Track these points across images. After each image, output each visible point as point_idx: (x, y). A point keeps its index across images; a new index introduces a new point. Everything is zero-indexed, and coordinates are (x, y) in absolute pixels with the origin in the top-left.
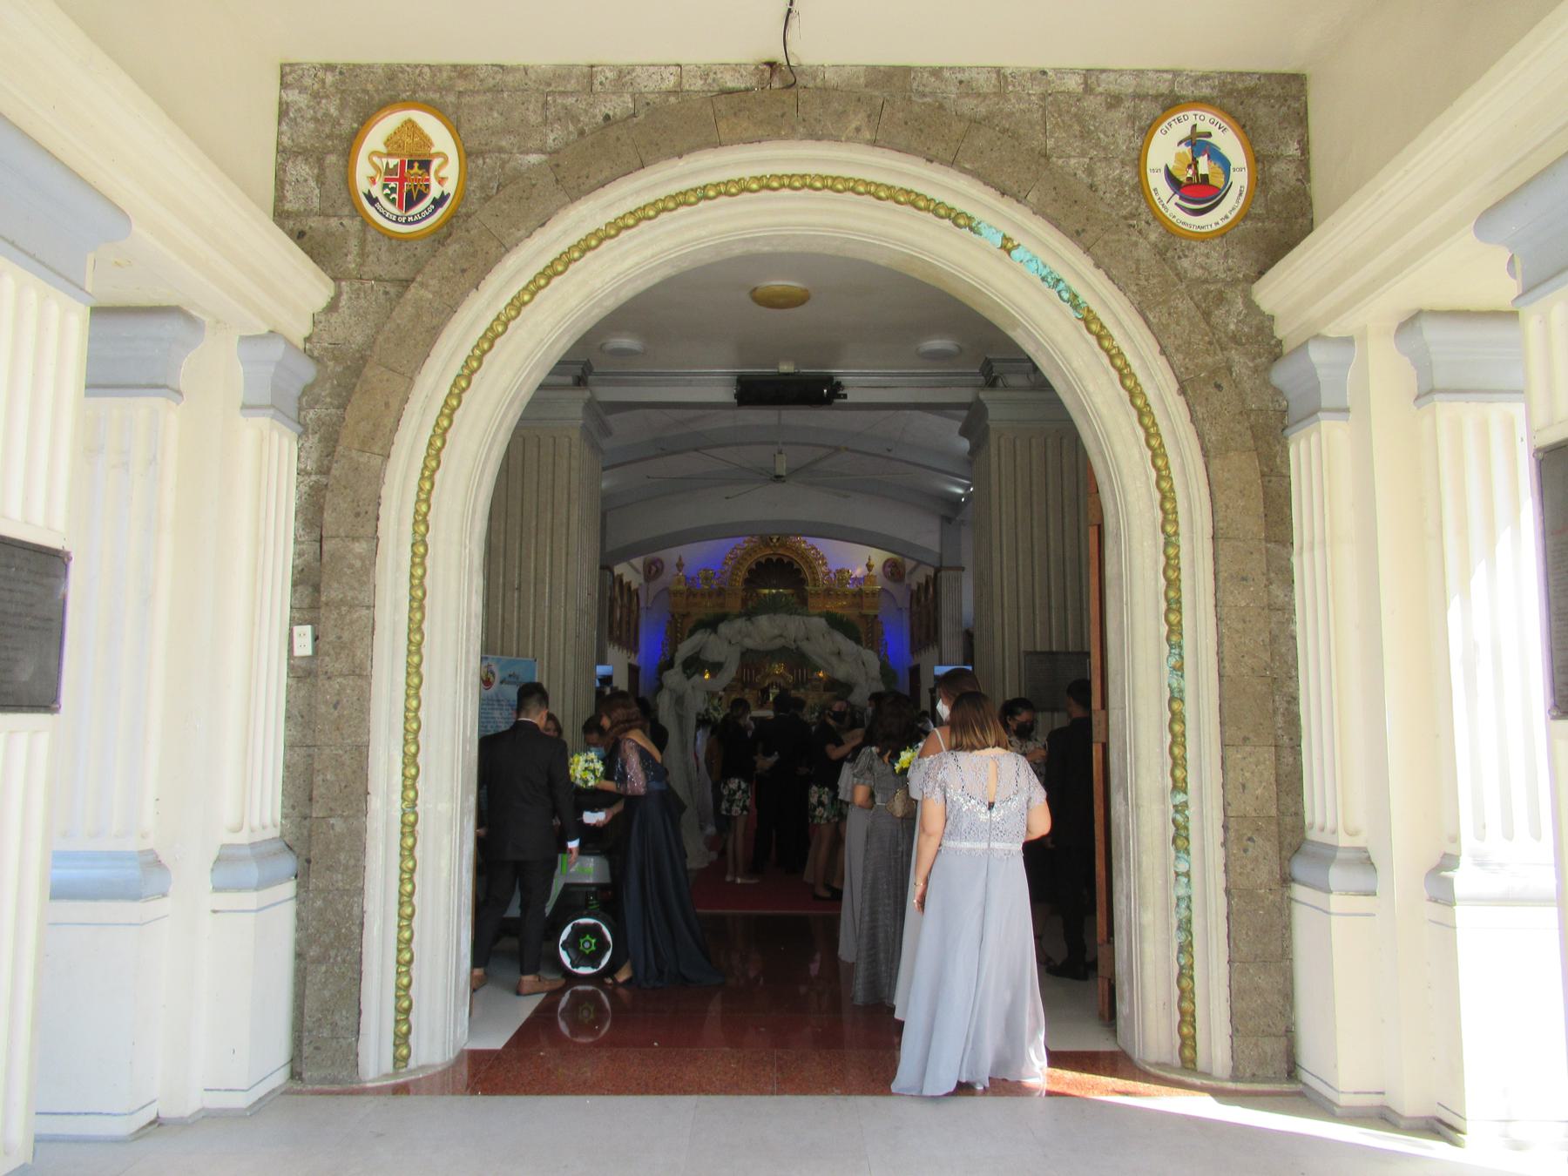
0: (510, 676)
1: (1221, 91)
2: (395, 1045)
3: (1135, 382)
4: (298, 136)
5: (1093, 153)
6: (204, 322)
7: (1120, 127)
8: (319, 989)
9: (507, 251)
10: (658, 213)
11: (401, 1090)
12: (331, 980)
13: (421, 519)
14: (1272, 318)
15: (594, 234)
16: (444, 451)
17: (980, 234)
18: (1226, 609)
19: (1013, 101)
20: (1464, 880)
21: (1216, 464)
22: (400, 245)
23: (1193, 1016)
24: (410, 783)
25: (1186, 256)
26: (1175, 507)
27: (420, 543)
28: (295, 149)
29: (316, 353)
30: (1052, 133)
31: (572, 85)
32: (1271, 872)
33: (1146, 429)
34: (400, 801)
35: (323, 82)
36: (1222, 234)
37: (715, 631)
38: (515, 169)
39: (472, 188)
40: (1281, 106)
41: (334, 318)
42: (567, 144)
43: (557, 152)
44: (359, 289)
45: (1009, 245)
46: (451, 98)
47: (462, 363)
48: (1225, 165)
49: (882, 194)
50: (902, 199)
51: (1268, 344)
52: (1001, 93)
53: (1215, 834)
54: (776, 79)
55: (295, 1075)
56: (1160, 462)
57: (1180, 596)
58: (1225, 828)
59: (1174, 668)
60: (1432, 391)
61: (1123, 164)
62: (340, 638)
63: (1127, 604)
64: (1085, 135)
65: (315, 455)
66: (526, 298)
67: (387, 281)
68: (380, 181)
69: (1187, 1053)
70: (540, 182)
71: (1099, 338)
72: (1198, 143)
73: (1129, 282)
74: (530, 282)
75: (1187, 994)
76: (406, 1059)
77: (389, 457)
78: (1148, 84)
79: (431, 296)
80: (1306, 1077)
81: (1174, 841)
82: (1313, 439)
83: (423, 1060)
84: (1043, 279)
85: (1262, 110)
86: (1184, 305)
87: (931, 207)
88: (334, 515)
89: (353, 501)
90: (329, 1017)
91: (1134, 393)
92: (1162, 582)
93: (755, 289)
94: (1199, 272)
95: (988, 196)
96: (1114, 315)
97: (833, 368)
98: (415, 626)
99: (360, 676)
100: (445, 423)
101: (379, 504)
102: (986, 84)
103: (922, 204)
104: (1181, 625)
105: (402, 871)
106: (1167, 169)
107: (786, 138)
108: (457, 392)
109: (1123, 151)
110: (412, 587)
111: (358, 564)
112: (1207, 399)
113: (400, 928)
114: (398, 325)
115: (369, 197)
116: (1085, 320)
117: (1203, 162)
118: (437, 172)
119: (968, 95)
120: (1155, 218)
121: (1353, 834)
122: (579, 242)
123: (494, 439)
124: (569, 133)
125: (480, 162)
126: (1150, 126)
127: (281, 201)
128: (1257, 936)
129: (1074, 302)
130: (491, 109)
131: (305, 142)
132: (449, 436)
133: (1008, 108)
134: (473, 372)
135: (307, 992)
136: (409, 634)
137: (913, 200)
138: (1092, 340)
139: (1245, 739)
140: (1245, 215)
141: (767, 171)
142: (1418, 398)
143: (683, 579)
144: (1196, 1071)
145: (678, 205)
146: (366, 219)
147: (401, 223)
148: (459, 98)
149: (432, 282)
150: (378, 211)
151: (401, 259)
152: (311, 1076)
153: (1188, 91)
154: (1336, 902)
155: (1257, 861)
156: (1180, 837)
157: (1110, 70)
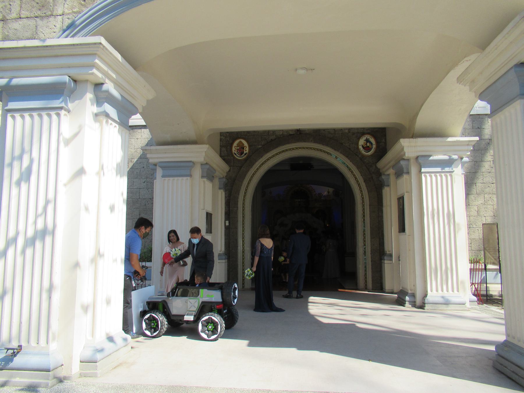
14: (380, 169)
24: (243, 245)
27: (243, 207)
35: (227, 135)
36: (371, 155)
46: (247, 137)
48: (372, 144)
53: (370, 252)
61: (355, 144)
69: (366, 287)
72: (367, 141)
84: (342, 163)
91: (357, 181)
103: (322, 151)
106: (362, 145)
115: (235, 153)
116: (349, 169)
121: (390, 251)
129: (347, 167)
137: (321, 150)
140: (375, 152)
141: (297, 147)
156: (365, 253)
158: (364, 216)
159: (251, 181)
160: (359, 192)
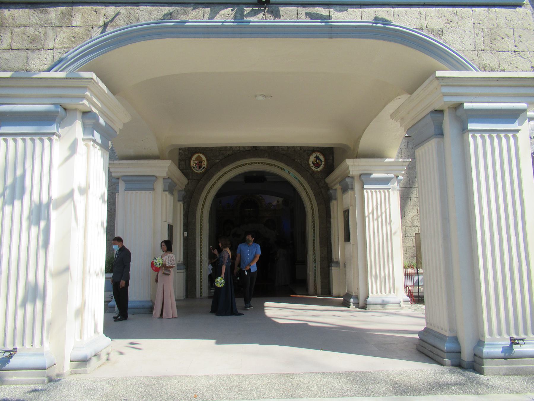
5: (301, 159)
13: (201, 215)
14: (328, 184)
24: (201, 255)
27: (201, 219)
36: (321, 171)
48: (321, 161)
69: (316, 292)
72: (317, 158)
81: (314, 262)
91: (308, 195)
92: (312, 223)
115: (193, 167)
116: (301, 184)
117: (318, 160)
121: (337, 259)
129: (299, 181)
137: (275, 166)
140: (324, 168)
141: (253, 162)
156: (315, 261)
158: (314, 227)
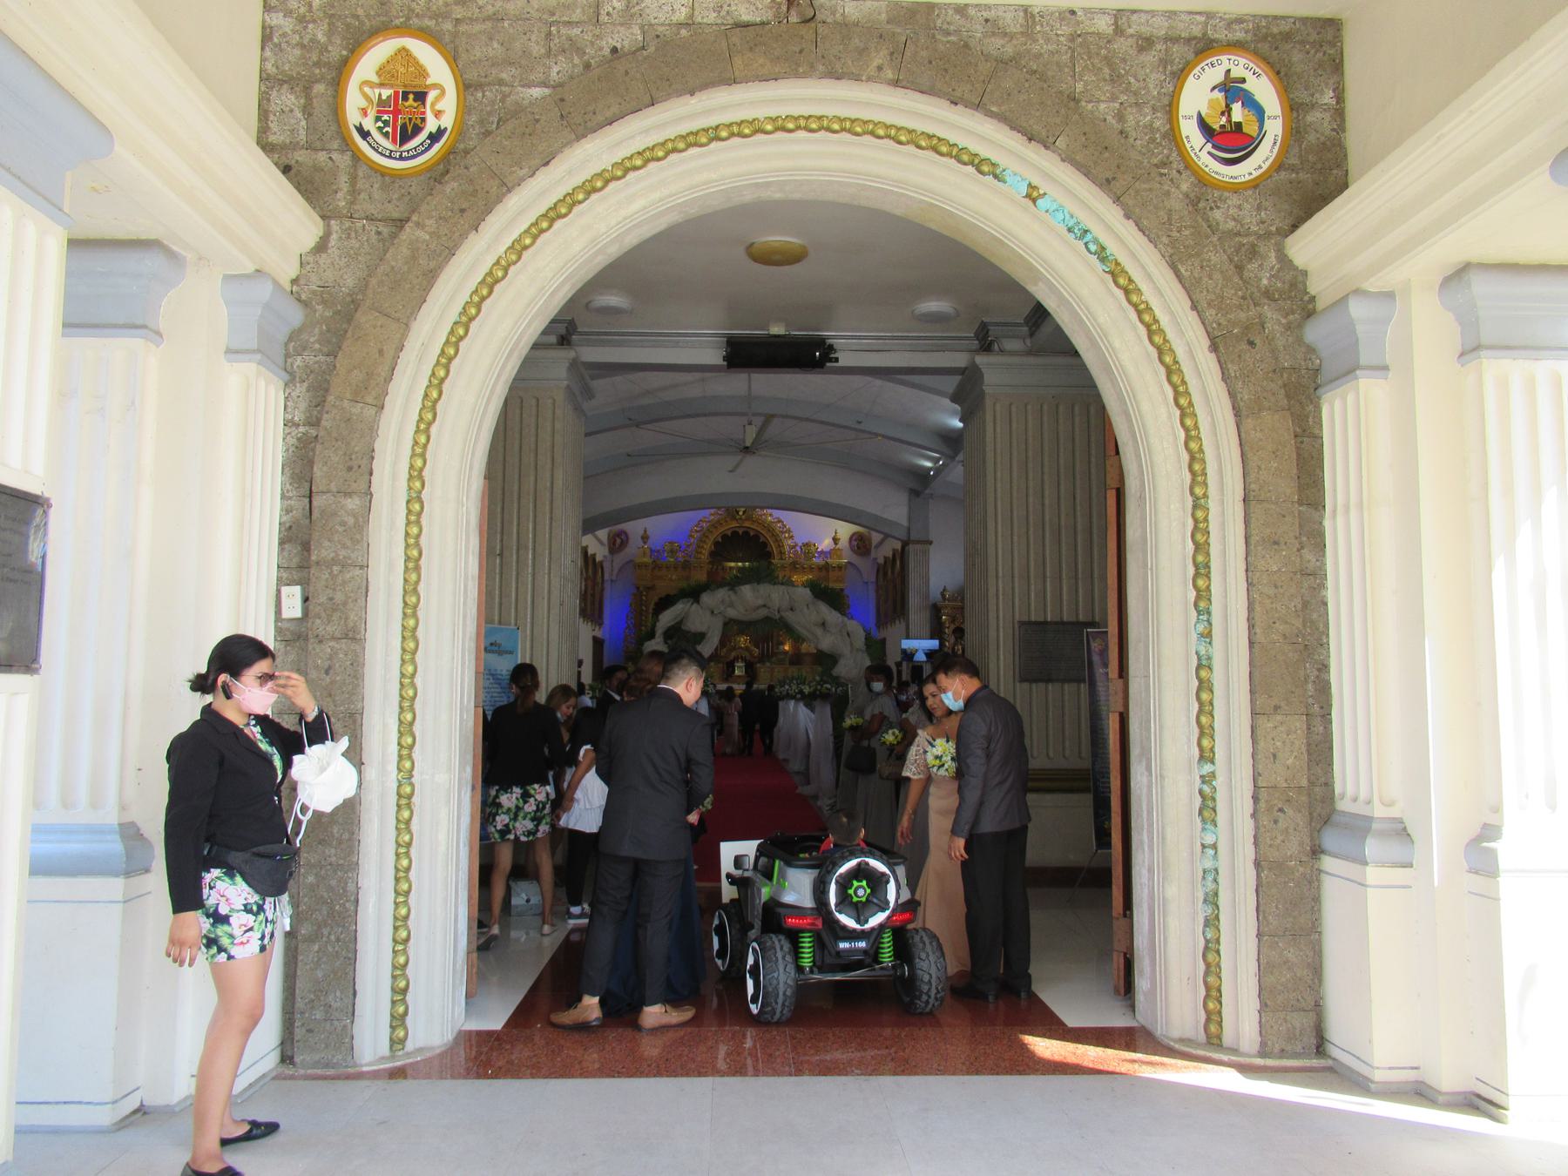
0: (492, 644)
1: (1255, 35)
2: (391, 1027)
3: (1164, 339)
4: (283, 64)
5: (1123, 98)
6: (185, 257)
7: (1151, 72)
8: (311, 969)
9: (509, 191)
10: (667, 154)
11: (398, 1074)
12: (324, 959)
14: (1305, 273)
15: (599, 175)
16: (440, 402)
17: (1005, 182)
18: (1258, 574)
19: (1041, 41)
20: (1506, 849)
21: (1249, 423)
22: (393, 182)
23: (1219, 991)
24: (406, 752)
25: (1218, 208)
26: (1204, 469)
27: (415, 499)
28: (280, 77)
29: (303, 297)
30: (1081, 76)
31: (577, 15)
32: (1301, 844)
33: (1175, 388)
34: (396, 771)
36: (1255, 185)
37: (697, 600)
38: (517, 103)
39: (470, 123)
40: (1316, 53)
41: (323, 259)
42: (572, 78)
43: (561, 85)
44: (350, 228)
45: (1035, 194)
46: (448, 26)
47: (460, 309)
48: (1260, 112)
49: (903, 138)
50: (923, 144)
51: (1301, 300)
52: (1028, 33)
54: (793, 12)
55: (286, 1058)
56: (1189, 422)
57: (1209, 561)
58: (1255, 798)
59: (1202, 635)
60: (1477, 348)
61: (1154, 109)
62: (331, 599)
63: (1152, 569)
64: (1115, 79)
65: (303, 405)
66: (528, 241)
67: (380, 221)
68: (372, 113)
69: (1213, 1028)
70: (544, 118)
71: (1127, 292)
72: (1231, 89)
73: (1160, 233)
74: (532, 225)
75: (1213, 969)
76: (403, 1041)
77: (383, 408)
78: (1181, 25)
79: (428, 237)
80: (1335, 1052)
81: (1200, 813)
82: (1350, 399)
83: (420, 1044)
84: (1070, 230)
85: (1297, 56)
86: (1216, 258)
87: (954, 153)
88: (325, 469)
89: (345, 454)
90: (322, 998)
92: (1190, 546)
93: (753, 244)
94: (1231, 224)
95: (1014, 141)
96: (1143, 267)
97: (827, 331)
98: (412, 587)
99: (354, 639)
100: (442, 373)
101: (373, 458)
102: (1012, 22)
103: (944, 149)
104: (1210, 591)
105: (398, 845)
106: (1199, 115)
107: (804, 76)
108: (455, 341)
109: (1154, 97)
110: (407, 546)
111: (351, 521)
112: (1240, 356)
113: (397, 904)
114: (393, 268)
115: (360, 130)
116: (1112, 273)
118: (433, 104)
119: (994, 34)
120: (1187, 167)
121: (1390, 804)
122: (584, 183)
123: (492, 392)
124: (574, 66)
125: (480, 95)
126: (1182, 71)
127: (265, 133)
128: (1287, 909)
129: (1101, 254)
130: (491, 39)
131: (290, 70)
132: (445, 387)
133: (1035, 48)
134: (472, 319)
135: (299, 973)
136: (404, 597)
137: (935, 145)
138: (1120, 294)
139: (1277, 708)
140: (1279, 166)
141: (783, 111)
142: (1462, 355)
143: (648, 551)
144: (1222, 1046)
145: (690, 145)
146: (358, 153)
147: (395, 158)
148: (456, 26)
149: (428, 222)
150: (370, 145)
151: (396, 196)
152: (304, 1059)
153: (1221, 35)
154: (1372, 874)
155: (1287, 832)
156: (1207, 808)
157: (1141, 11)
158: (1202, 570)
159: (474, 326)
160: (1170, 416)
